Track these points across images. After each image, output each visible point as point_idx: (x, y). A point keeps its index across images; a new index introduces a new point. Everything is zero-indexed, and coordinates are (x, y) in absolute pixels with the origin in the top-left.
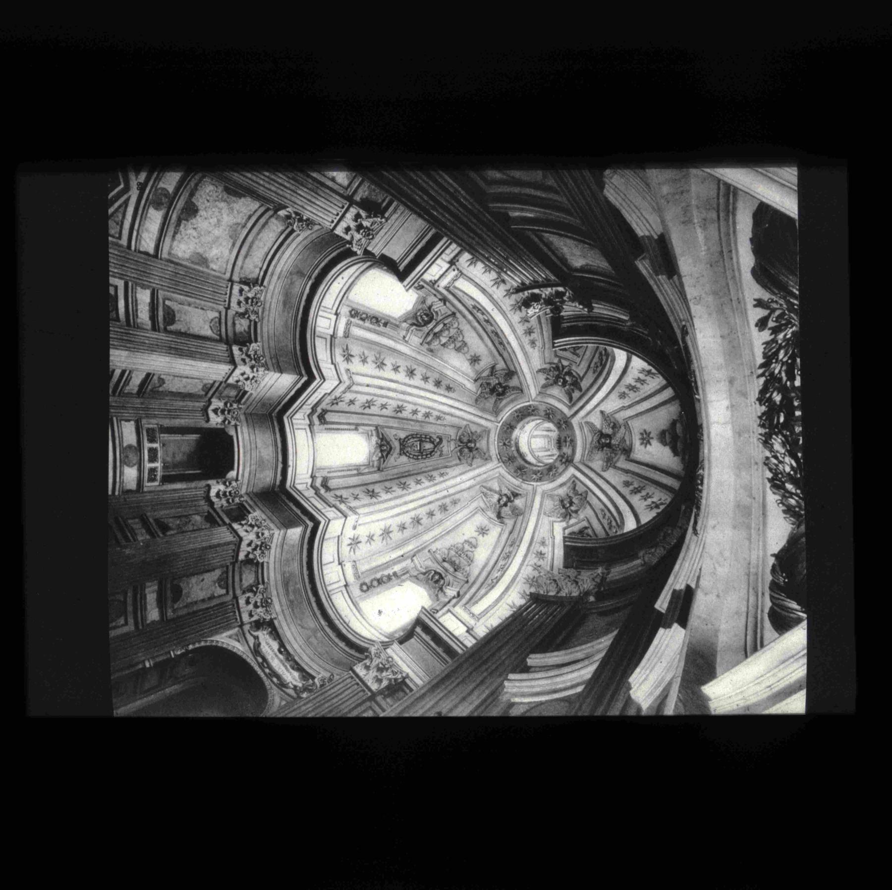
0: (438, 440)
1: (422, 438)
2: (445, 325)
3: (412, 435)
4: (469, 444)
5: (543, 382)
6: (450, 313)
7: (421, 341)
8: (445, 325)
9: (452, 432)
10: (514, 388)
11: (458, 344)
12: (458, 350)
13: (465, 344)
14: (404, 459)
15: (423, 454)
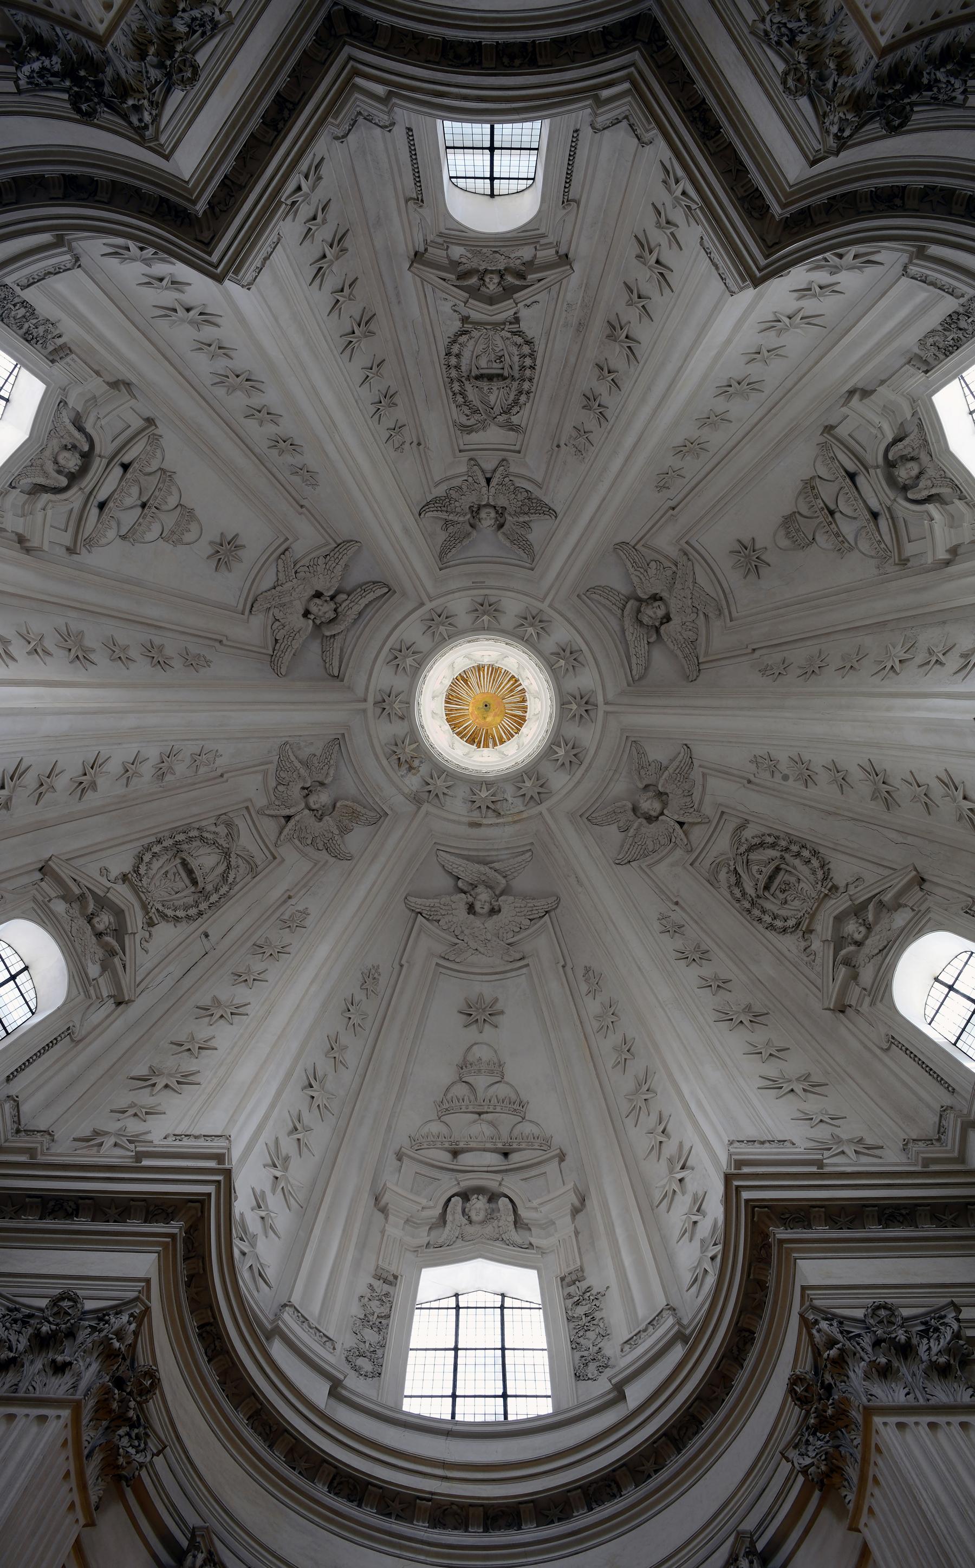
0: (222, 830)
1: (176, 847)
2: (125, 467)
3: (148, 849)
4: (312, 799)
5: (442, 536)
6: (137, 423)
7: (67, 539)
8: (125, 467)
9: (252, 788)
10: (363, 587)
11: (169, 520)
12: (173, 537)
13: (187, 514)
14: (165, 933)
15: (204, 896)
